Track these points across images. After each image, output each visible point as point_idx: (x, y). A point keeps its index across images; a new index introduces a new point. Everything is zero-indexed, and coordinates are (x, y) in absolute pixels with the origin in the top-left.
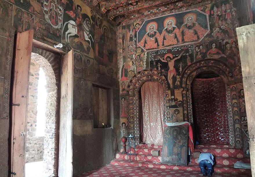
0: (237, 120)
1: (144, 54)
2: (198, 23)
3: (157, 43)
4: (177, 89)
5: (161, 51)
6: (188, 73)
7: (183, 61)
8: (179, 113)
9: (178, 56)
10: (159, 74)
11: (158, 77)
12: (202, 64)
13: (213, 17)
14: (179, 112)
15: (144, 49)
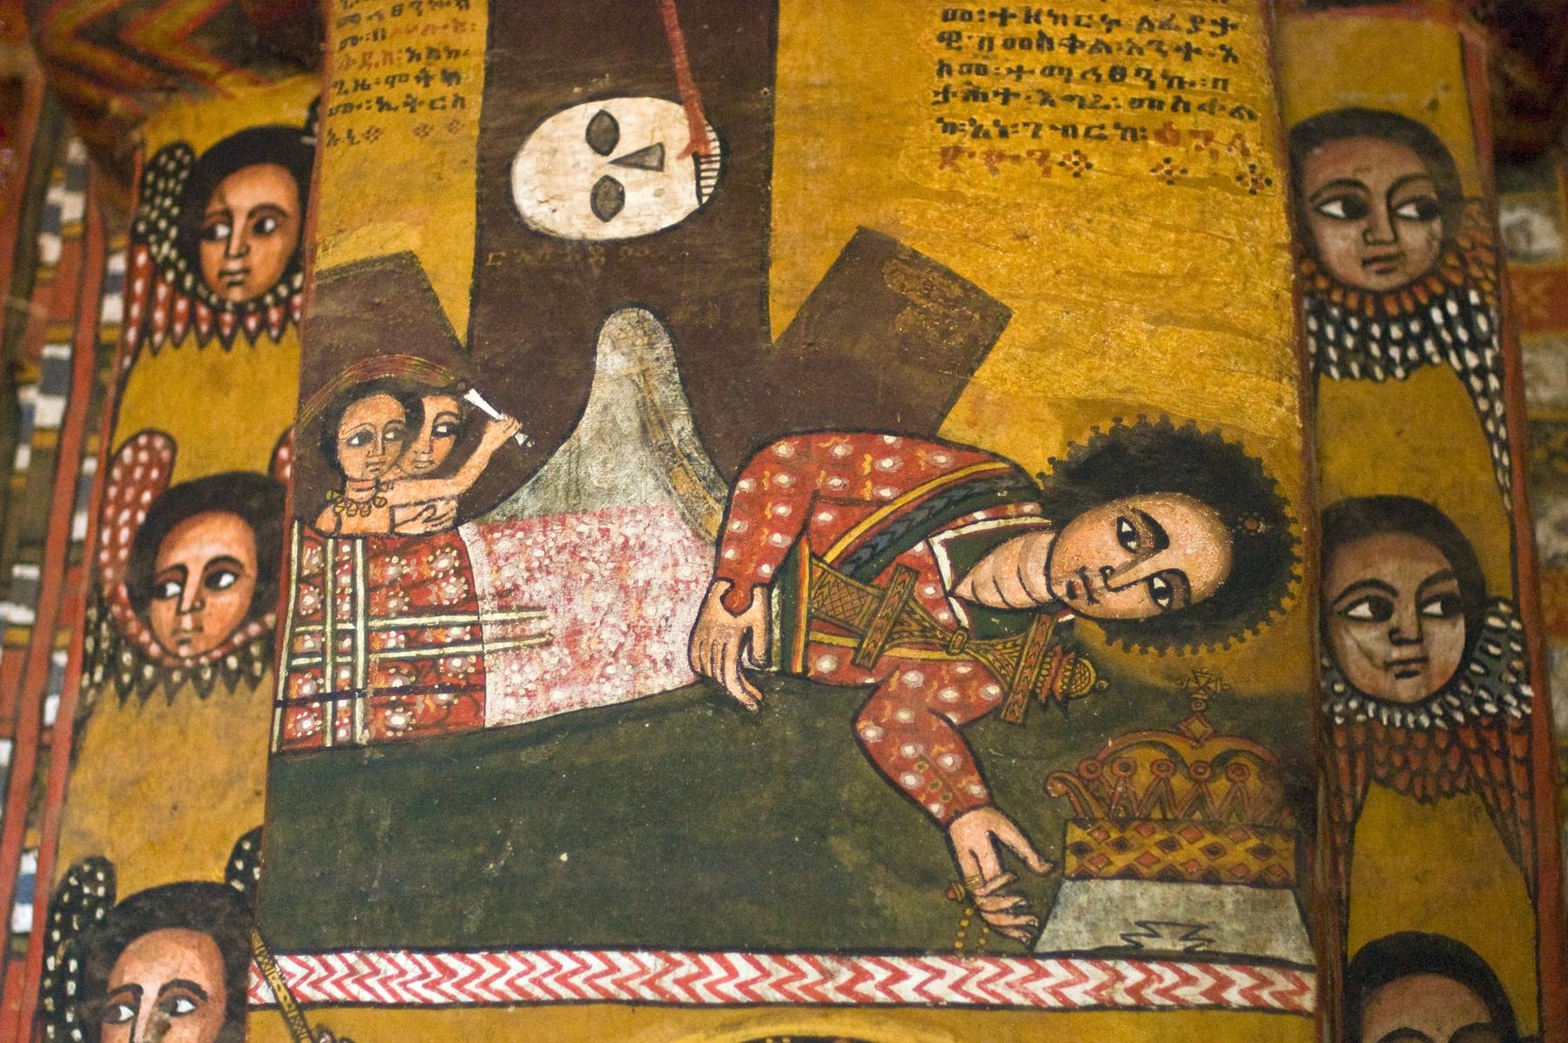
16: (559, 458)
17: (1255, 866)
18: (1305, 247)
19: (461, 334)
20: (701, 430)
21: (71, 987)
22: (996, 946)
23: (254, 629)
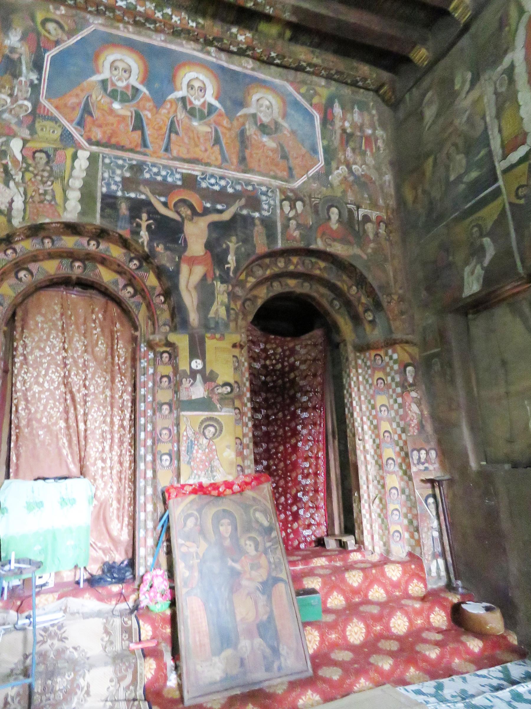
0: (390, 461)
1: (75, 157)
2: (290, 126)
3: (139, 132)
4: (218, 336)
5: (155, 170)
6: (249, 285)
7: (239, 233)
8: (219, 431)
9: (220, 212)
10: (131, 260)
11: (117, 276)
12: (293, 264)
13: (331, 128)
14: (221, 431)
15: (77, 136)
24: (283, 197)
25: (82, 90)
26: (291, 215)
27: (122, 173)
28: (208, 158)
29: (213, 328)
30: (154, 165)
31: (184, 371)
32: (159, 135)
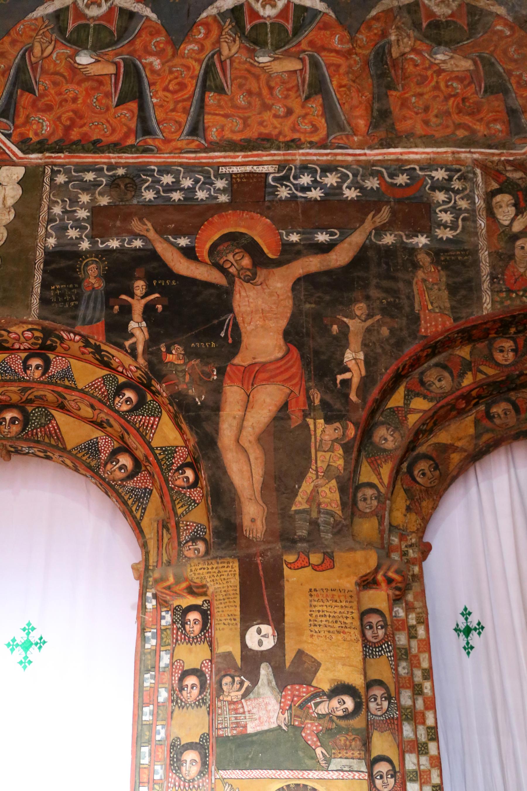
2: (511, 10)
3: (134, 106)
4: (315, 558)
5: (167, 179)
6: (413, 419)
7: (374, 293)
9: (325, 248)
10: (119, 390)
11: (97, 433)
16: (256, 688)
17: (359, 756)
18: (363, 635)
19: (240, 666)
20: (277, 684)
21: (175, 760)
22: (322, 769)
23: (200, 697)
24: (495, 186)
25: (14, 42)
26: (517, 227)
27: (93, 200)
28: (294, 129)
29: (302, 539)
30: (165, 169)
31: (228, 655)
32: (177, 102)
